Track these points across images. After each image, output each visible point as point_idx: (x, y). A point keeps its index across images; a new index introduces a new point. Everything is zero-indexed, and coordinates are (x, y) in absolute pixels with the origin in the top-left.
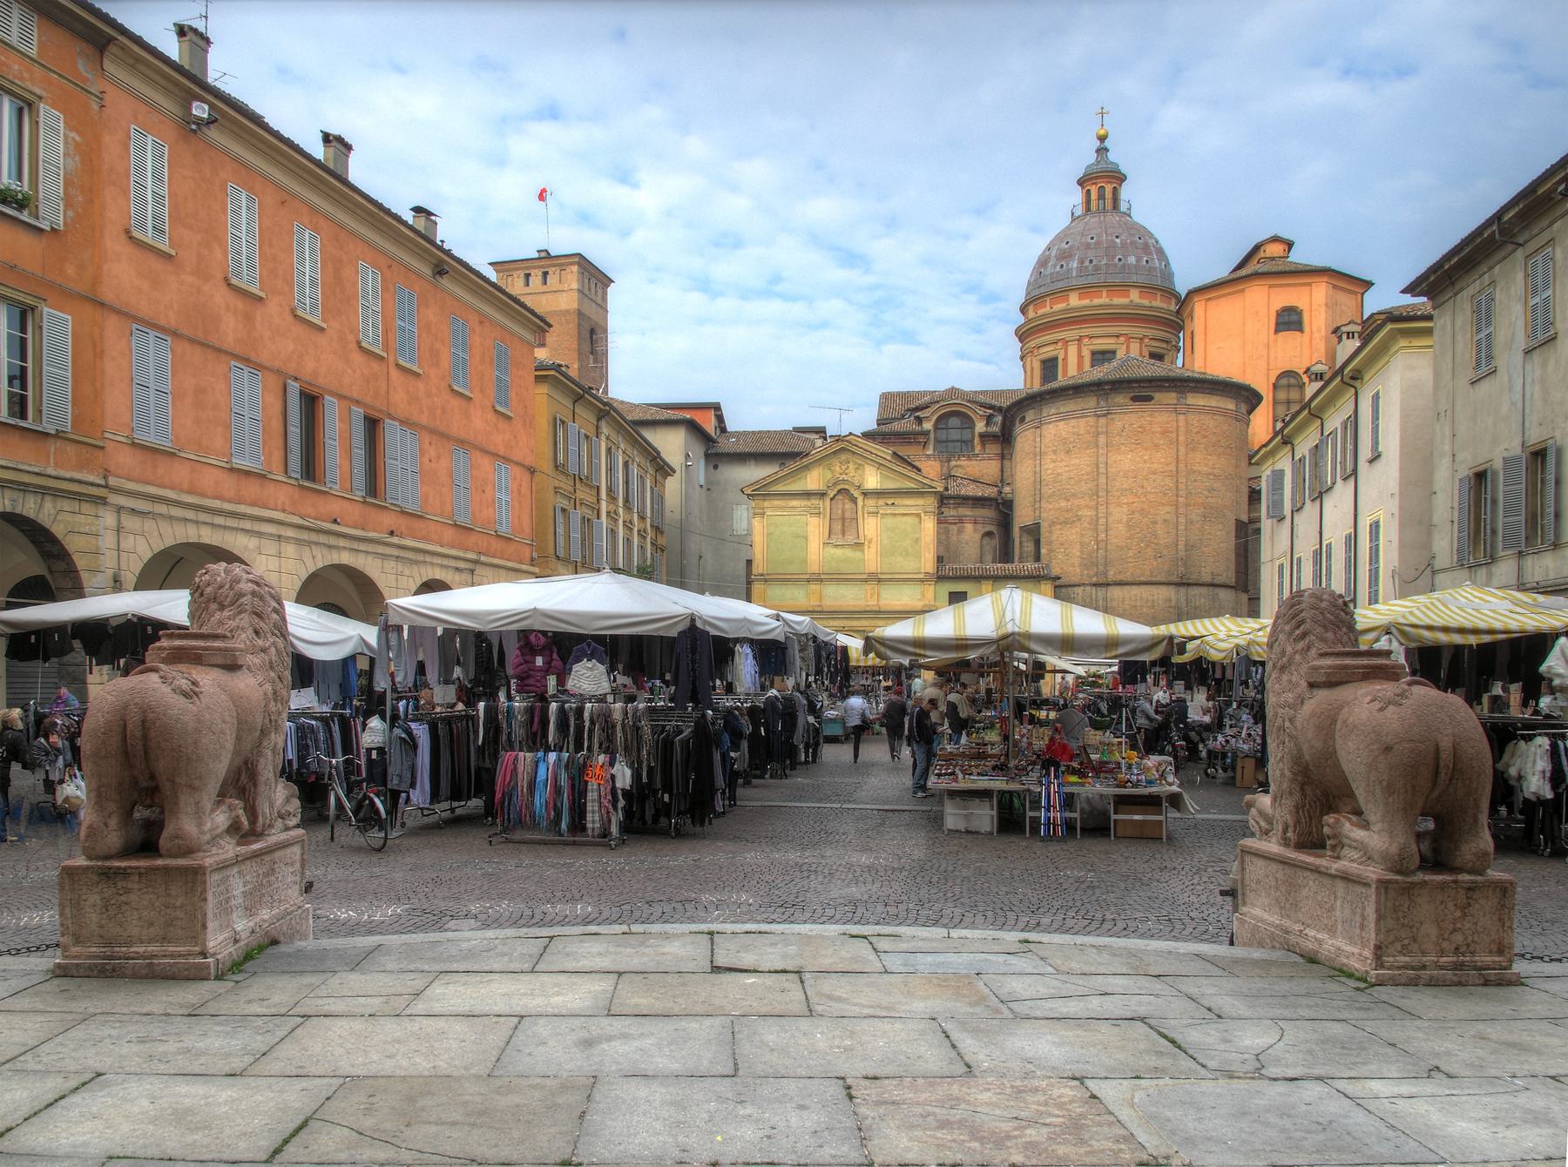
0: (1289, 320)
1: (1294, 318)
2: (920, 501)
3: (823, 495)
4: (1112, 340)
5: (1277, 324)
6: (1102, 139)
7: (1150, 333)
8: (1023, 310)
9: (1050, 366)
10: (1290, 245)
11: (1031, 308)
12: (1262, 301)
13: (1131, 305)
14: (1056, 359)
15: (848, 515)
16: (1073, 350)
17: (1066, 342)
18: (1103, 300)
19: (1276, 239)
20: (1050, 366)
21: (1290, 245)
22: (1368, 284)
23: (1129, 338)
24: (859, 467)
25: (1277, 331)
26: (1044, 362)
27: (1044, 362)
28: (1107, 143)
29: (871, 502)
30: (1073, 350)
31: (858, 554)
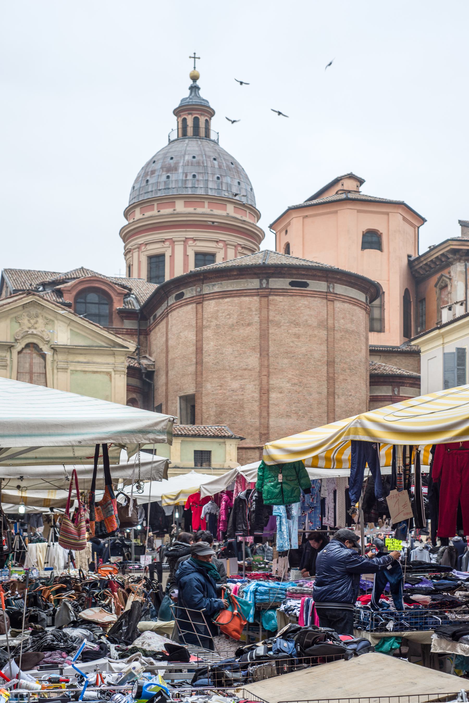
0: (372, 240)
1: (375, 239)
2: (110, 360)
3: (10, 347)
4: (214, 245)
5: (363, 242)
6: (195, 78)
7: (242, 242)
8: (127, 213)
9: (156, 262)
10: (361, 182)
11: (138, 210)
12: (354, 223)
13: (228, 217)
14: (163, 255)
15: (36, 369)
16: (179, 249)
17: (173, 242)
19: (351, 176)
20: (156, 262)
21: (361, 182)
22: (424, 220)
23: (226, 245)
24: (48, 322)
25: (363, 248)
26: (150, 258)
27: (150, 258)
28: (198, 83)
29: (60, 357)
30: (179, 249)
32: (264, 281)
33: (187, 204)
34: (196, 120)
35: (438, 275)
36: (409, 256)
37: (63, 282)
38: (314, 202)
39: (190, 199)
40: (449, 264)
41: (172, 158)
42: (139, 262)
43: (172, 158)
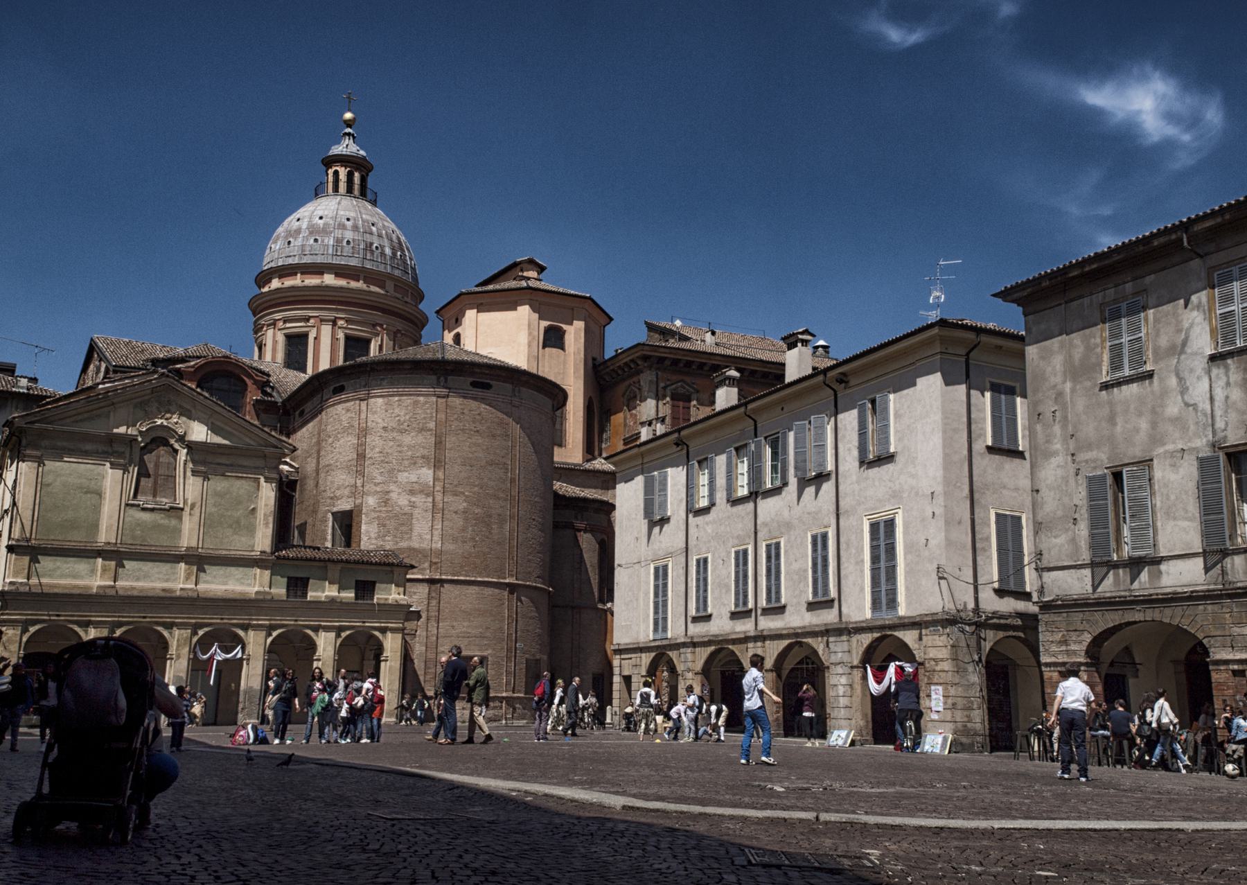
18: (360, 285)
22: (611, 319)
31: (174, 522)
32: (442, 378)
33: (337, 275)
34: (350, 176)
35: (627, 383)
36: (594, 359)
37: (183, 360)
38: (491, 287)
39: (340, 271)
40: (639, 372)
41: (321, 218)
42: (275, 342)
43: (321, 218)
